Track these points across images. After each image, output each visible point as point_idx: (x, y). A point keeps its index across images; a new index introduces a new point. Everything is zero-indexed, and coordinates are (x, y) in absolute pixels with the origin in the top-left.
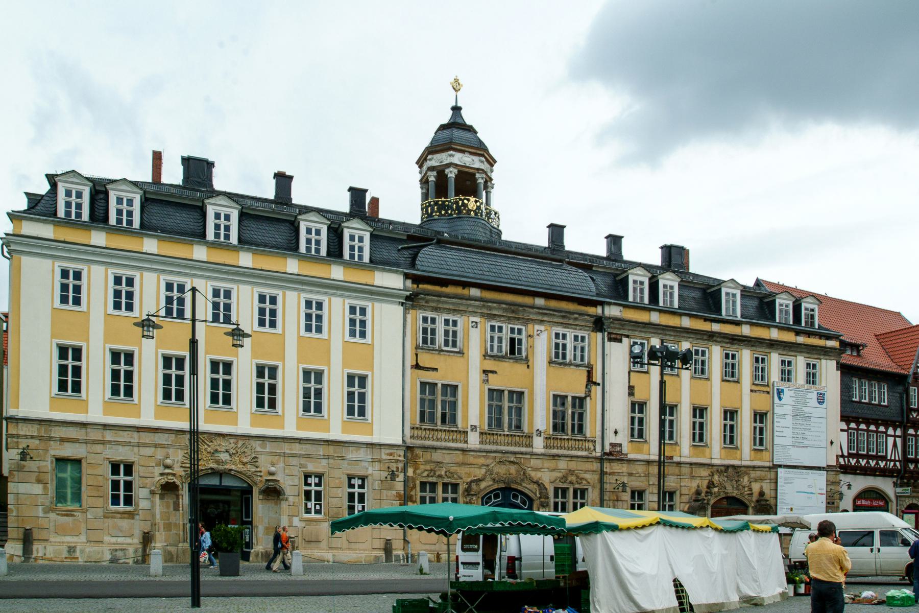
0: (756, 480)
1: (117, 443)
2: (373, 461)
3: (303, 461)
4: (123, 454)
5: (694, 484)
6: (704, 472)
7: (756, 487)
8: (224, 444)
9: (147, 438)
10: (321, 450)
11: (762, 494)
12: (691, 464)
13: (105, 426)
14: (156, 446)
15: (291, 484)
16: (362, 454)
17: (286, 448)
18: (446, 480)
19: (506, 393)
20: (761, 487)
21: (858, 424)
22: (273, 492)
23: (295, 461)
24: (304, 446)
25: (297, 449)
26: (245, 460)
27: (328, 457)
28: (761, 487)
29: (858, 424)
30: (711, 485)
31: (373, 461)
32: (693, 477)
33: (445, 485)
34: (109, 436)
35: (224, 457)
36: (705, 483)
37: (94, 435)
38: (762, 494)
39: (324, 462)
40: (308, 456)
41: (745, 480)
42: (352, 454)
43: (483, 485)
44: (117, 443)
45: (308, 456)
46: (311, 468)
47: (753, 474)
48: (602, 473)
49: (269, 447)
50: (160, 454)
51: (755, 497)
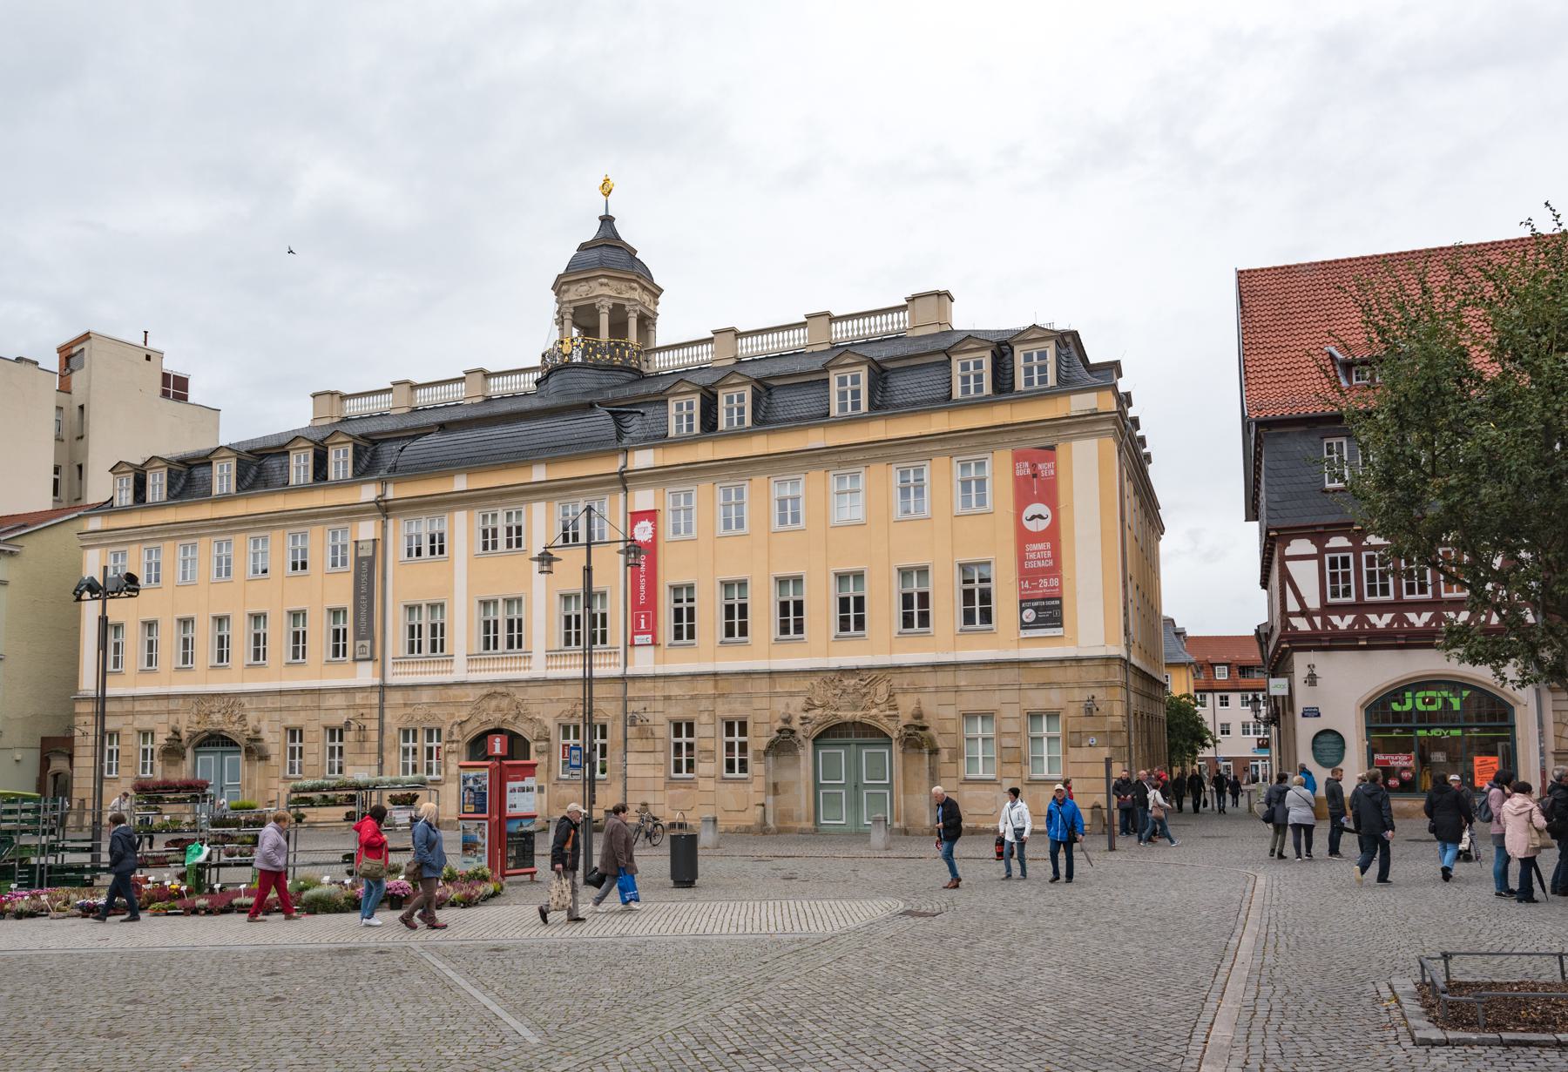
0: (905, 691)
1: (142, 713)
2: (348, 707)
3: (285, 714)
4: (146, 722)
5: (780, 707)
6: (804, 684)
7: (907, 705)
8: (217, 704)
9: (163, 705)
10: (300, 701)
11: (919, 716)
12: (771, 673)
13: (134, 698)
14: (169, 712)
15: (274, 741)
16: (339, 700)
17: (269, 702)
18: (426, 725)
19: (500, 602)
20: (919, 702)
21: (1357, 537)
22: (254, 750)
23: (276, 716)
24: (285, 699)
25: (278, 702)
26: (234, 719)
27: (304, 708)
28: (919, 702)
29: (1357, 537)
30: (810, 706)
31: (348, 707)
32: (772, 695)
33: (430, 732)
34: (138, 706)
35: (216, 717)
36: (799, 702)
37: (128, 706)
38: (919, 716)
39: (302, 714)
40: (288, 709)
41: (882, 689)
42: (331, 701)
43: (468, 728)
44: (142, 713)
45: (288, 709)
46: (292, 721)
47: (898, 681)
48: (626, 701)
49: (256, 702)
50: (173, 718)
51: (906, 719)
